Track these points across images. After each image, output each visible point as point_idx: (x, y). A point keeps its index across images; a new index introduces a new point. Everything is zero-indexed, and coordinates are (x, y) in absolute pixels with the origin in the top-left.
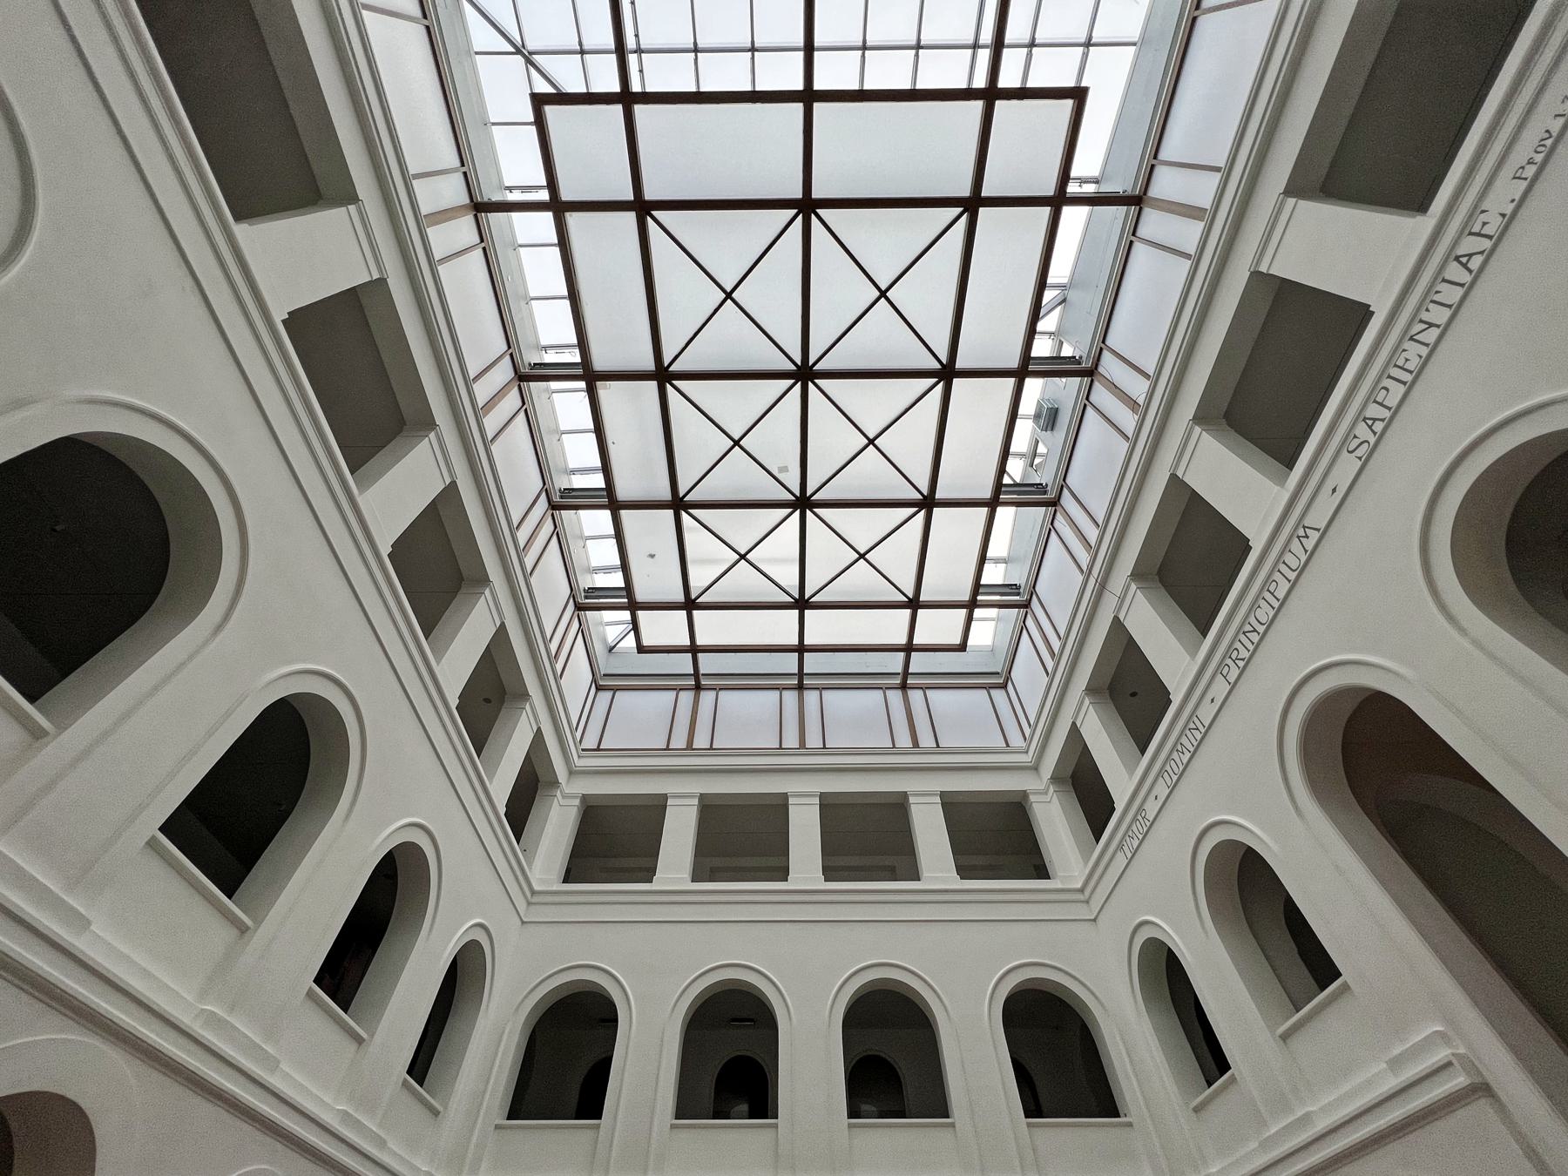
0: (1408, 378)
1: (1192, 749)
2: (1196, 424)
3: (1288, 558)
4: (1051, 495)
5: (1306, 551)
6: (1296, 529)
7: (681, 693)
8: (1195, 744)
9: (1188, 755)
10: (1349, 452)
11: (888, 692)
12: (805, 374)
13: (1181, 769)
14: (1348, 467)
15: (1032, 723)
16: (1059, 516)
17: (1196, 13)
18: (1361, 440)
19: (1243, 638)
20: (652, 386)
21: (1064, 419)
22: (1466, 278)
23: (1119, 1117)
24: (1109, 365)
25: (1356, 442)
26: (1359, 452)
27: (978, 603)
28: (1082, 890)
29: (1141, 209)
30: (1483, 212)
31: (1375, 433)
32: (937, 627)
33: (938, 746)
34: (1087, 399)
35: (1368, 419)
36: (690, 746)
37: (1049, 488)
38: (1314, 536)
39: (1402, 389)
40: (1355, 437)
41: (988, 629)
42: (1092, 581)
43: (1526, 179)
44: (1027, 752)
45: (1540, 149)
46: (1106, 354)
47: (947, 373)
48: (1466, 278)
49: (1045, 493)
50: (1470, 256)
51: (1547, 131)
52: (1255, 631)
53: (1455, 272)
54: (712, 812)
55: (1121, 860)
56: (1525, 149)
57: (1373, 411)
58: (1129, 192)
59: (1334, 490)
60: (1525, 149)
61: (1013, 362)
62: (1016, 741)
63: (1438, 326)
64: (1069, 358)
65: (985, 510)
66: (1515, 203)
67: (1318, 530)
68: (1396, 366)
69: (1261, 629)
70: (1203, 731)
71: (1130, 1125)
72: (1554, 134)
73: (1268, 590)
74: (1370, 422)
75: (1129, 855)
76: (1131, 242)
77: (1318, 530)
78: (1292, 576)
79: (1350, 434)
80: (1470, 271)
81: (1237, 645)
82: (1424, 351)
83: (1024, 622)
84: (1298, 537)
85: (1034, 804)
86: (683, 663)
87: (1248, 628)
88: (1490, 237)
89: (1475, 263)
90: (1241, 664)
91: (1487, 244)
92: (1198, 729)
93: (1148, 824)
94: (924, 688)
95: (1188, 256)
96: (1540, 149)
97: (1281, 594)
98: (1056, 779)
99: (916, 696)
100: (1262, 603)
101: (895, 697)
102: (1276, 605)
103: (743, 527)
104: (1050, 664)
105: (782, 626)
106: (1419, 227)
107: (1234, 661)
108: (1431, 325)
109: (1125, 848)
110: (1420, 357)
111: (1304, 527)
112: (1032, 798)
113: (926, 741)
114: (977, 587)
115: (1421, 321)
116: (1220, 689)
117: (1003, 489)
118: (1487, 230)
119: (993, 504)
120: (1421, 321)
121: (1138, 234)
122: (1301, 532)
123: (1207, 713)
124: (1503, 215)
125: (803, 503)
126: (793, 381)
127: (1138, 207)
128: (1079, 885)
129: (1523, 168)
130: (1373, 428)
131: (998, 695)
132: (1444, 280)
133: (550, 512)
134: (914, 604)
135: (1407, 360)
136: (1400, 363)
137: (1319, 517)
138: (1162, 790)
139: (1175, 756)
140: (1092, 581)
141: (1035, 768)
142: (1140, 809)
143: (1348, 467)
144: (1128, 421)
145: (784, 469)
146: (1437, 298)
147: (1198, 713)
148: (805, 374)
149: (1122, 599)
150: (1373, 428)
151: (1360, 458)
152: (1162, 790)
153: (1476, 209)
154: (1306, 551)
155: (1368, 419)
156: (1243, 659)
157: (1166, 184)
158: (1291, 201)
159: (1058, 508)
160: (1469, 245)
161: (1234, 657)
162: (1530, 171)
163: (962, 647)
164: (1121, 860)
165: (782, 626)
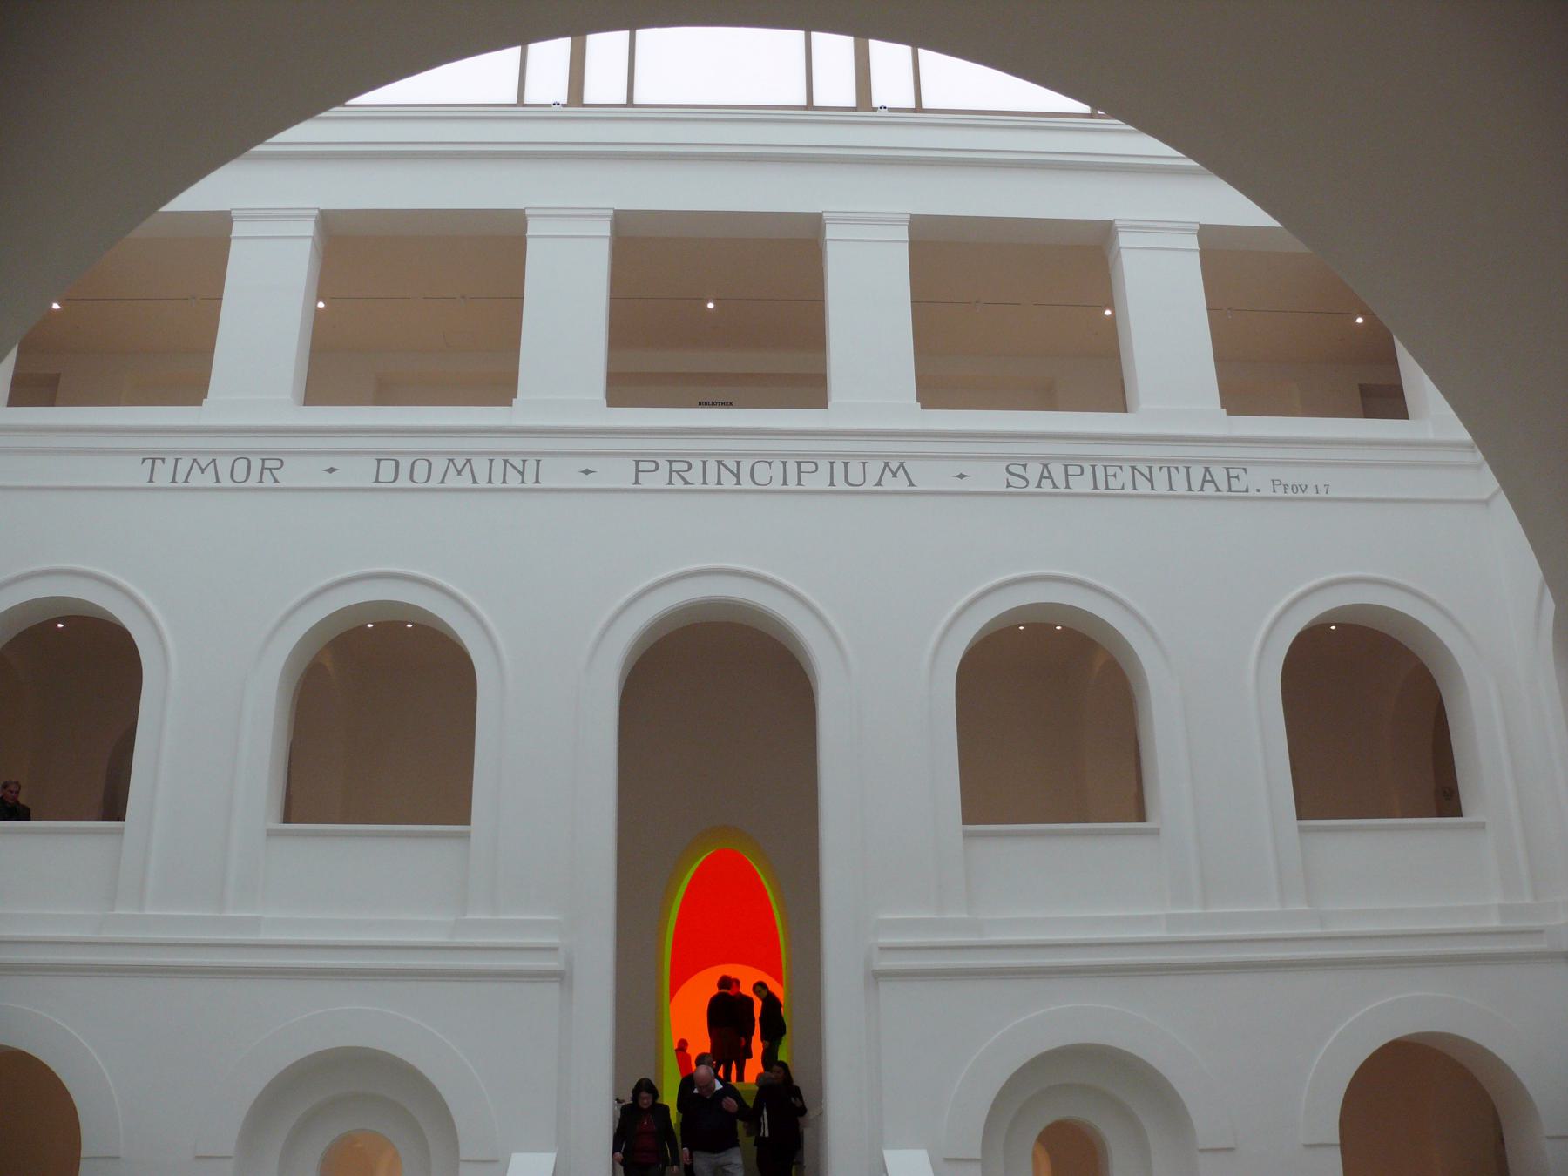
5: (879, 484)
10: (1007, 468)
13: (428, 485)
19: (712, 466)
25: (1019, 470)
26: (1014, 481)
30: (1245, 469)
31: (1039, 486)
35: (1048, 471)
38: (901, 484)
39: (1089, 489)
40: (1025, 466)
51: (1306, 486)
52: (737, 476)
56: (1290, 476)
57: (1057, 470)
59: (961, 476)
67: (911, 484)
68: (1105, 467)
69: (750, 486)
74: (1046, 475)
77: (911, 484)
81: (697, 464)
84: (886, 465)
92: (522, 474)
97: (810, 482)
100: (777, 464)
107: (671, 471)
108: (1151, 481)
111: (902, 465)
115: (1150, 468)
116: (618, 473)
120: (1150, 468)
122: (894, 465)
123: (556, 474)
132: (1188, 468)
135: (1115, 476)
136: (1111, 471)
139: (439, 464)
143: (992, 477)
146: (1173, 471)
150: (1043, 480)
155: (1048, 471)
156: (687, 483)
160: (1219, 473)
161: (676, 466)
162: (1280, 492)
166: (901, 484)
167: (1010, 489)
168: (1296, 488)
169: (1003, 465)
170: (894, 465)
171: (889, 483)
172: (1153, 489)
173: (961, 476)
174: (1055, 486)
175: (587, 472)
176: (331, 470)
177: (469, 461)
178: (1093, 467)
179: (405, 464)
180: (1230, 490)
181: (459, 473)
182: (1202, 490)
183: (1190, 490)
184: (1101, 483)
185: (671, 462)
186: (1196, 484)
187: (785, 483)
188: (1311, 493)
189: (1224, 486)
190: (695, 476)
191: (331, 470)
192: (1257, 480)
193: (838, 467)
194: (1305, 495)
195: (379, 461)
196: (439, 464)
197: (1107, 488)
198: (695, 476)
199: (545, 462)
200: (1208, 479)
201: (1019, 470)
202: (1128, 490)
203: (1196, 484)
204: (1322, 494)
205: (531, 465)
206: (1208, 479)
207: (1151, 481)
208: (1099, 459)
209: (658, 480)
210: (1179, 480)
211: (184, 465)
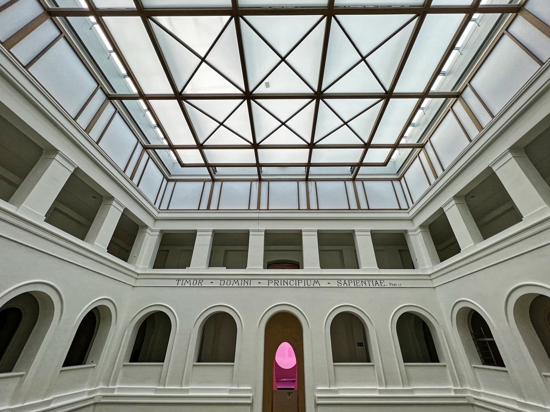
3: (309, 281)
19: (282, 281)
26: (339, 284)
31: (344, 285)
40: (341, 281)
52: (287, 283)
57: (347, 282)
59: (329, 283)
67: (320, 285)
79: (341, 280)
81: (280, 281)
87: (286, 281)
90: (276, 286)
92: (247, 283)
108: (365, 284)
109: (180, 282)
111: (318, 281)
116: (264, 283)
122: (316, 281)
123: (254, 284)
136: (357, 282)
139: (232, 281)
143: (334, 284)
146: (370, 281)
154: (313, 285)
156: (278, 285)
160: (378, 282)
161: (276, 282)
162: (391, 286)
167: (338, 286)
168: (395, 285)
170: (316, 281)
171: (316, 285)
172: (366, 286)
173: (329, 283)
174: (347, 285)
175: (259, 283)
176: (212, 283)
177: (238, 281)
178: (354, 281)
179: (226, 281)
180: (381, 286)
181: (236, 283)
182: (376, 286)
183: (373, 286)
184: (356, 285)
185: (275, 281)
186: (374, 284)
187: (296, 285)
188: (397, 286)
189: (380, 285)
190: (279, 284)
191: (212, 283)
192: (386, 283)
194: (397, 286)
195: (221, 281)
196: (232, 281)
197: (357, 285)
198: (279, 284)
199: (252, 280)
200: (377, 283)
201: (340, 282)
202: (361, 286)
203: (374, 284)
204: (400, 286)
205: (249, 281)
206: (377, 283)
207: (365, 284)
209: (272, 285)
210: (371, 283)
211: (185, 281)
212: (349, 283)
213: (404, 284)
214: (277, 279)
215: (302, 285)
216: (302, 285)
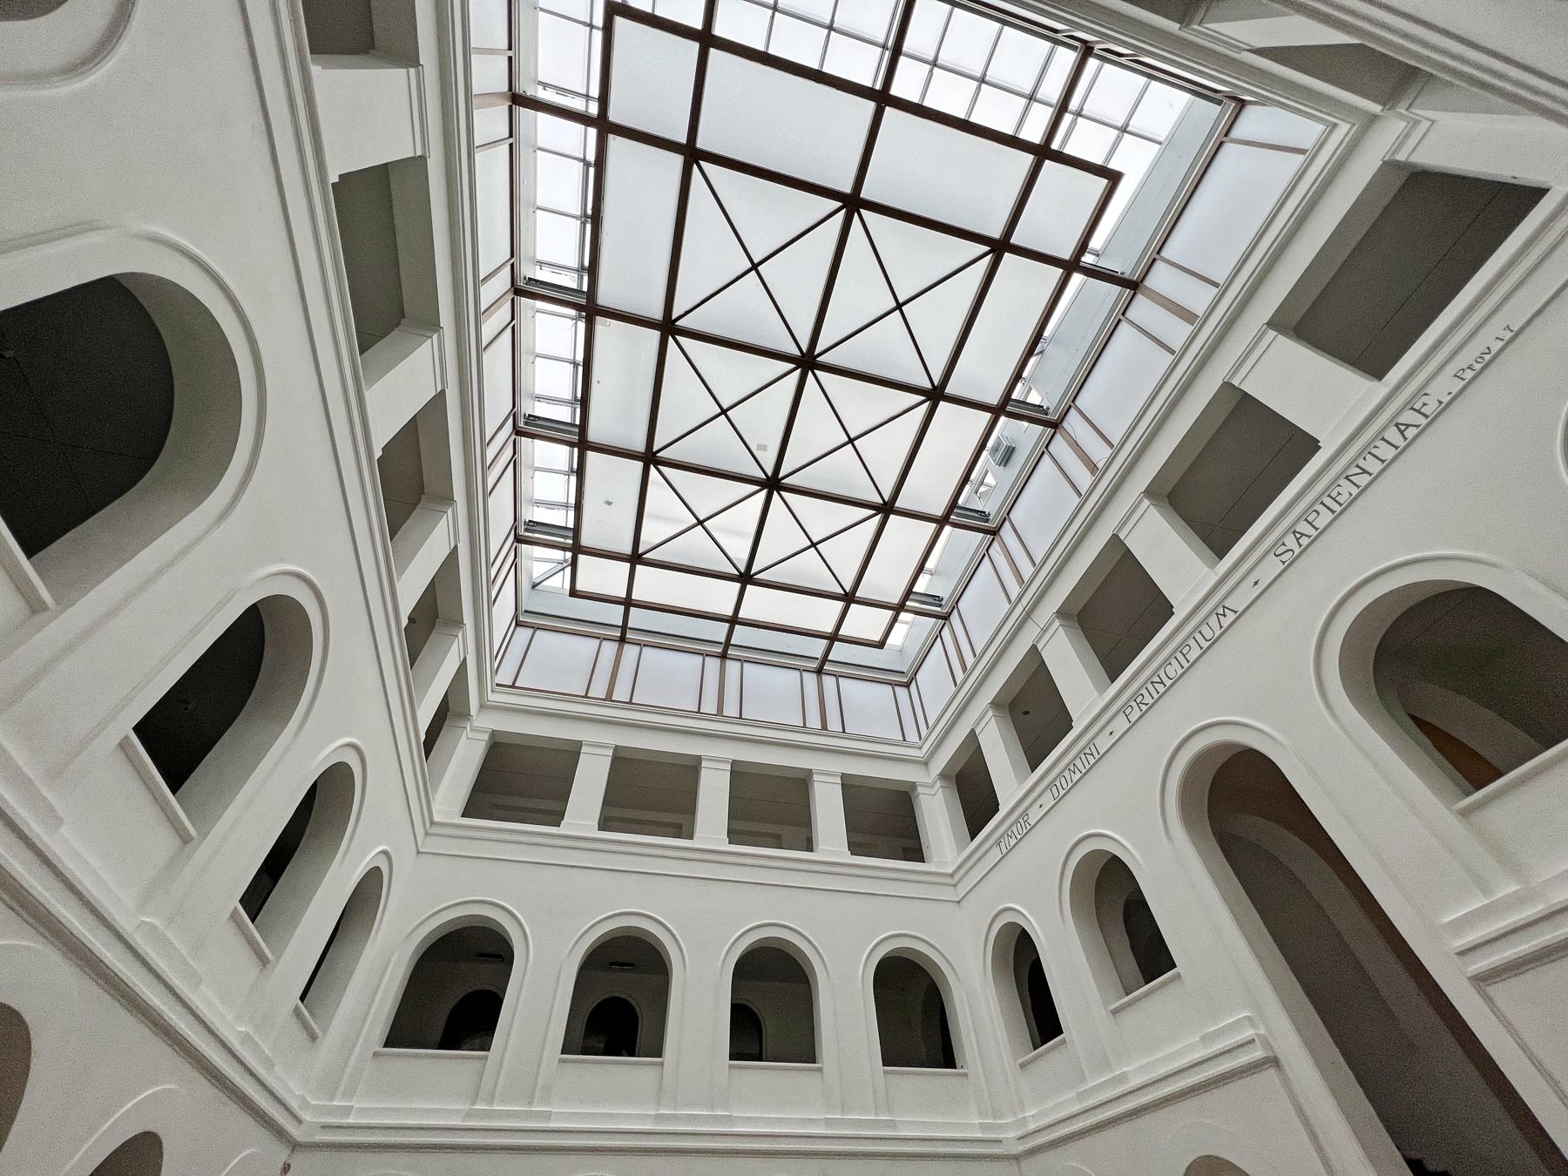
0: (1338, 509)
1: (1084, 771)
2: (1148, 498)
3: (1205, 629)
4: (992, 525)
5: (1221, 627)
6: (1217, 607)
7: (604, 643)
8: (1088, 767)
9: (1079, 775)
11: (804, 674)
12: (807, 362)
14: (1273, 566)
15: (930, 726)
16: (995, 544)
17: (1225, 139)
18: (1287, 548)
20: (655, 335)
21: (1019, 460)
22: (1401, 443)
23: (956, 1068)
24: (1073, 423)
25: (1283, 549)
26: (1284, 558)
27: (906, 608)
28: (952, 875)
29: (1135, 293)
30: (1426, 394)
31: (1300, 546)
32: (864, 623)
33: (844, 732)
34: (1047, 447)
35: (1300, 533)
36: (609, 697)
37: (991, 517)
38: (1231, 617)
39: (1330, 516)
40: (1283, 544)
41: (908, 631)
42: (1019, 609)
43: (1463, 379)
44: (920, 748)
45: (1479, 360)
46: (1073, 411)
47: (936, 395)
48: (1401, 443)
49: (987, 521)
50: (1408, 426)
51: (1488, 348)
52: (1162, 683)
53: (1392, 434)
54: (624, 764)
55: (995, 855)
56: (1467, 357)
57: (1303, 527)
58: (1126, 276)
59: (1256, 583)
60: (1467, 357)
61: (994, 399)
62: (912, 736)
63: (1370, 474)
64: (1038, 406)
65: (933, 526)
66: (1452, 395)
67: (1236, 612)
68: (1329, 496)
70: (1097, 757)
71: (966, 1075)
72: (1493, 353)
73: (1181, 652)
74: (1299, 536)
75: (1004, 851)
76: (1120, 320)
77: (1236, 612)
78: (1205, 645)
79: (1280, 542)
80: (1405, 439)
81: (1144, 691)
82: (1355, 491)
83: (940, 632)
84: (1217, 614)
85: (921, 795)
86: (615, 614)
87: (1156, 679)
88: (1426, 416)
89: (1411, 433)
90: (1144, 708)
91: (1423, 421)
93: (1029, 827)
94: (837, 676)
95: (1172, 352)
96: (1479, 360)
97: (1192, 656)
98: (943, 776)
99: (829, 682)
100: (1173, 661)
101: (810, 679)
102: (1186, 665)
103: (708, 494)
104: (960, 676)
105: (721, 597)
106: (1375, 391)
108: (1365, 471)
109: (1002, 845)
110: (1351, 495)
111: (1224, 607)
112: (920, 790)
113: (834, 724)
114: (909, 592)
115: (1358, 466)
116: (1120, 724)
117: (955, 510)
118: (1425, 410)
119: (942, 521)
120: (1358, 466)
121: (1127, 315)
122: (1220, 611)
123: (1103, 743)
124: (1440, 403)
125: (773, 484)
126: (794, 366)
127: (1133, 292)
128: (950, 871)
129: (1463, 370)
130: (1300, 541)
131: (901, 692)
132: (1383, 439)
133: (513, 437)
134: (849, 598)
135: (1339, 494)
136: (1334, 494)
137: (1238, 602)
138: (1048, 801)
139: (1066, 773)
140: (1019, 609)
141: (926, 763)
142: (1025, 813)
143: (1273, 566)
144: (1084, 479)
145: (763, 448)
146: (1374, 451)
147: (1096, 741)
148: (807, 362)
149: (1044, 631)
151: (1284, 563)
152: (1048, 801)
153: (1421, 391)
154: (1221, 627)
157: (1161, 279)
158: (1272, 334)
159: (997, 538)
160: (1408, 417)
161: (1138, 701)
162: (1469, 375)
163: (880, 645)
164: (995, 855)
165: (721, 597)
166: (1231, 617)
169: (1272, 554)
170: (1220, 611)
176: (1041, 806)
178: (1322, 503)
191: (1041, 806)
193: (1198, 637)
196: (1066, 773)
200: (1401, 429)
204: (1508, 335)
208: (1321, 495)
212: (1310, 523)
213: (1515, 314)
214: (1137, 693)
215: (1194, 653)
216: (1194, 653)
